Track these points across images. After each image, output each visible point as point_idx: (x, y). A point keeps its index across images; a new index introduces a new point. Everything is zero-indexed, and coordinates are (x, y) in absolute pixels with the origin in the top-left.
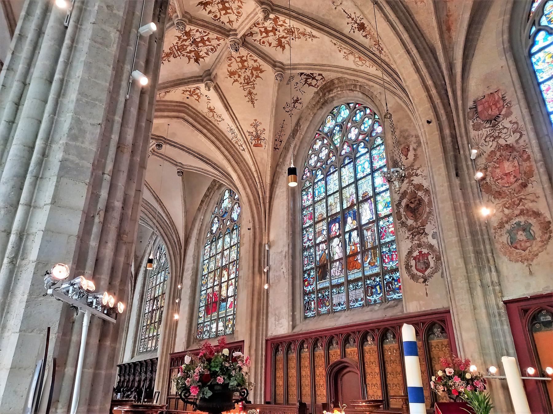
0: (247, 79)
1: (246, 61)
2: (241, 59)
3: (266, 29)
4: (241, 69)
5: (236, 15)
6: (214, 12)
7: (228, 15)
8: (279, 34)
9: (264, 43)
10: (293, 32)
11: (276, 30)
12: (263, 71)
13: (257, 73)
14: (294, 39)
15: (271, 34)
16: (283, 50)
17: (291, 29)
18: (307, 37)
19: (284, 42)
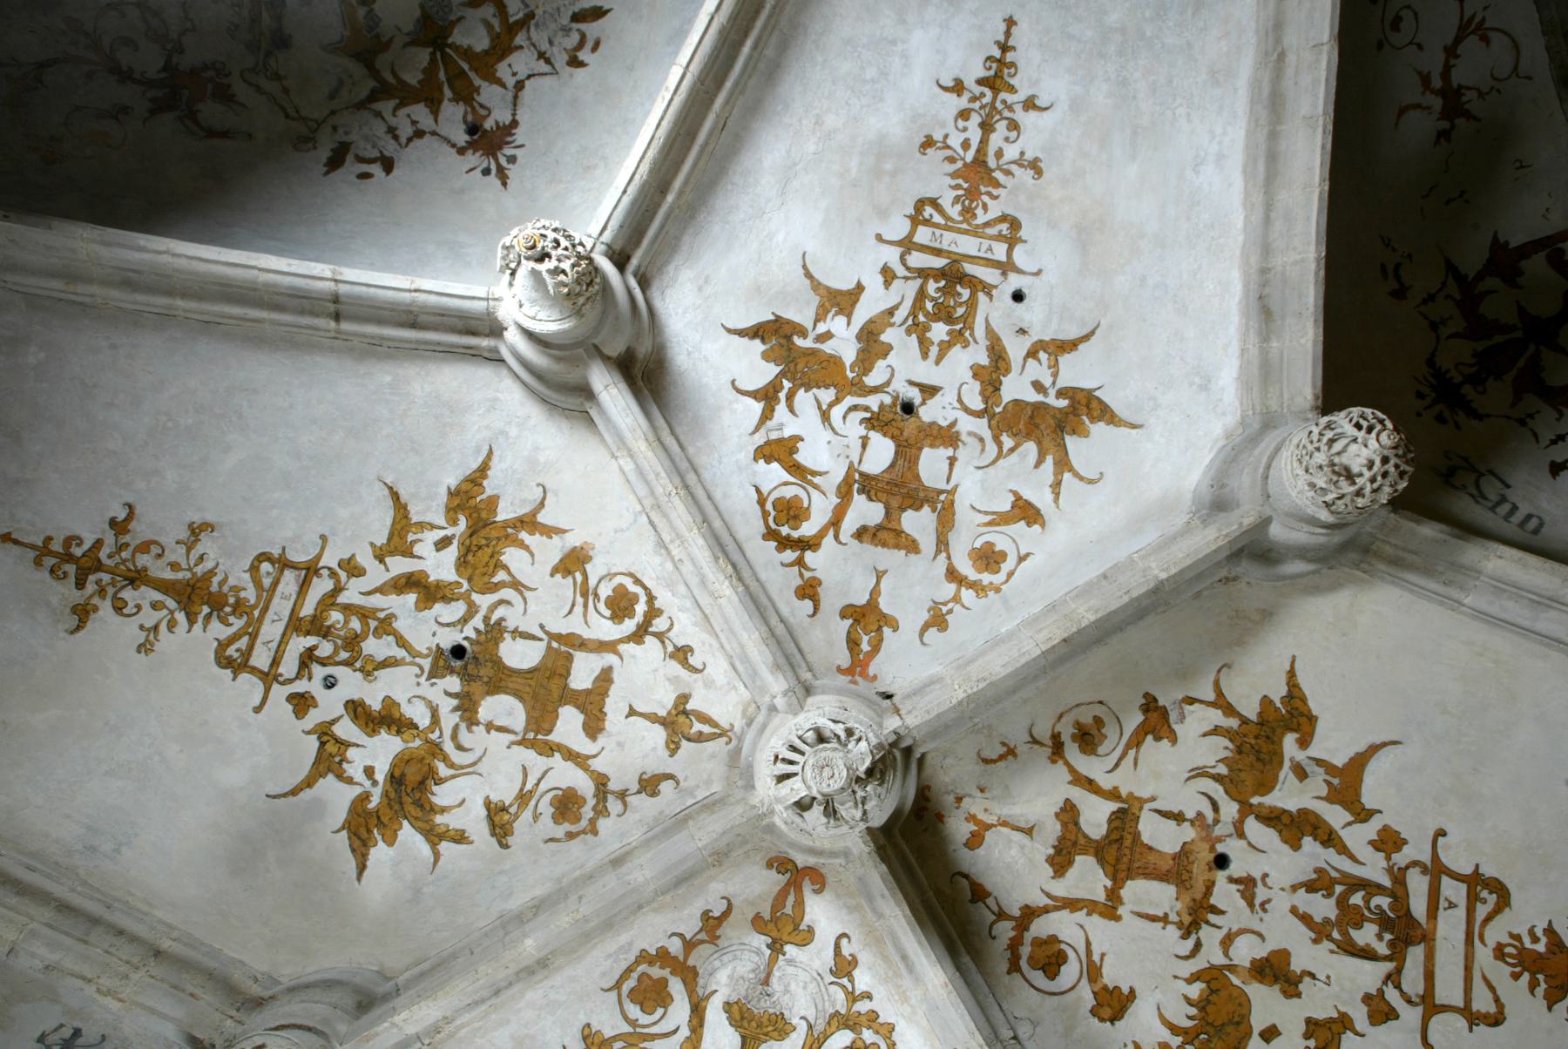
0: (1350, 917)
1: (1124, 819)
2: (1099, 850)
3: (860, 483)
4: (1198, 914)
5: (638, 636)
6: (523, 797)
7: (614, 706)
8: (947, 398)
9: (988, 558)
10: (953, 275)
11: (908, 408)
12: (1294, 693)
13: (1301, 773)
14: (1015, 282)
15: (931, 465)
16: (1105, 414)
17: (924, 274)
18: (1011, 152)
19: (1038, 386)
